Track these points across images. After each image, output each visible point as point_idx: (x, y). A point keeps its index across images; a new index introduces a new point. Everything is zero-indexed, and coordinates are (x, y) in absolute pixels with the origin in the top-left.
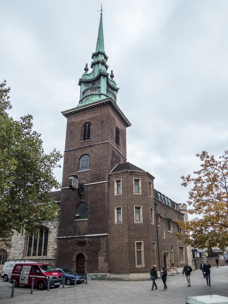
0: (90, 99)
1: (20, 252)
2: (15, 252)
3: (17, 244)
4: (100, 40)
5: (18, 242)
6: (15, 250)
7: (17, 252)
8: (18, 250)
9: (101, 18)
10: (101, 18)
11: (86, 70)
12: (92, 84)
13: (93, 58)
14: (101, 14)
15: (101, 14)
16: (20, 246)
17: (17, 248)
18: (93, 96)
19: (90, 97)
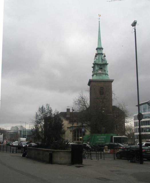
11: (96, 56)
13: (97, 49)
14: (99, 22)
15: (99, 22)
16: (71, 137)
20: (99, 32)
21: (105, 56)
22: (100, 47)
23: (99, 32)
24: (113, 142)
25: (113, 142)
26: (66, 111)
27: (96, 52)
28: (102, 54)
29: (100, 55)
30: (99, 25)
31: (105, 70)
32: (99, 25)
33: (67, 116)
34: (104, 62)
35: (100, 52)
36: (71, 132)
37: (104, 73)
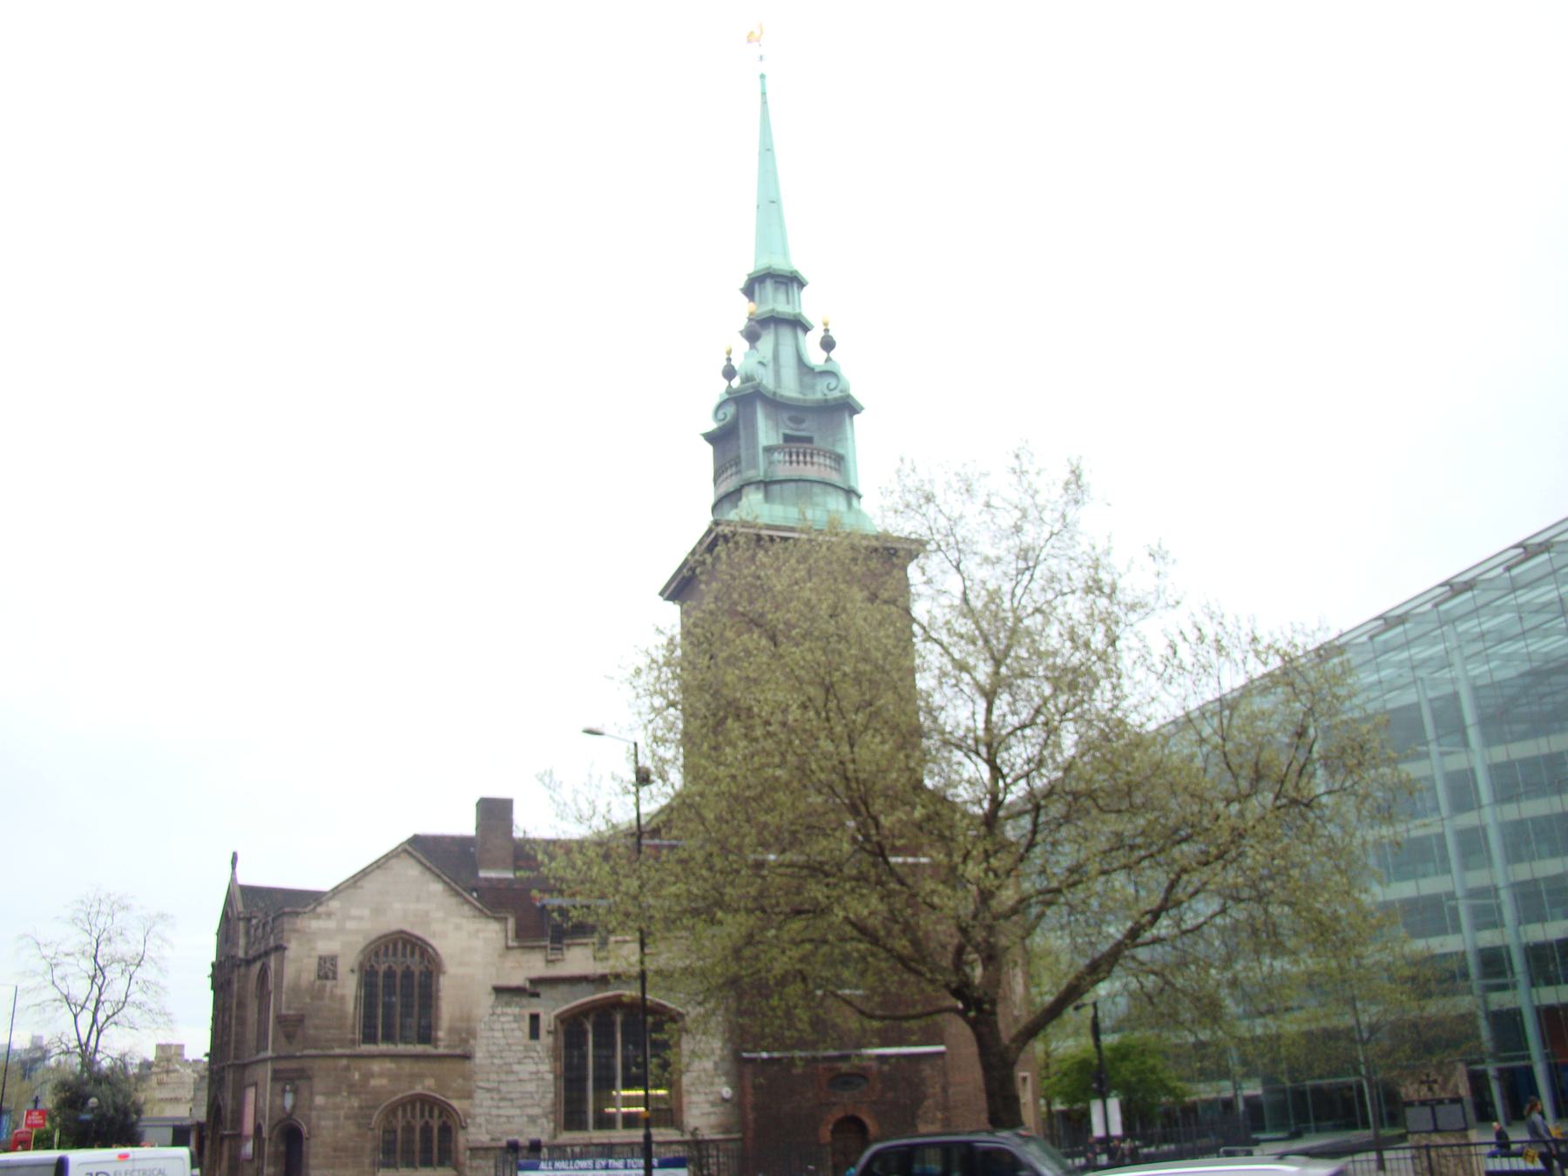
0: (819, 499)
1: (536, 1111)
2: (502, 1112)
3: (512, 1078)
4: (770, 204)
5: (516, 1068)
6: (502, 1104)
7: (517, 1112)
8: (517, 1103)
9: (764, 94)
10: (764, 94)
12: (792, 419)
16: (531, 1087)
17: (513, 1096)
18: (830, 489)
19: (817, 489)
20: (767, 150)
21: (828, 344)
22: (779, 264)
23: (767, 150)
24: (941, 1048)
25: (941, 1048)
26: (466, 825)
27: (742, 310)
28: (798, 324)
29: (786, 334)
30: (764, 102)
31: (839, 460)
32: (764, 102)
33: (483, 874)
34: (821, 391)
35: (782, 307)
36: (534, 1033)
37: (834, 477)
